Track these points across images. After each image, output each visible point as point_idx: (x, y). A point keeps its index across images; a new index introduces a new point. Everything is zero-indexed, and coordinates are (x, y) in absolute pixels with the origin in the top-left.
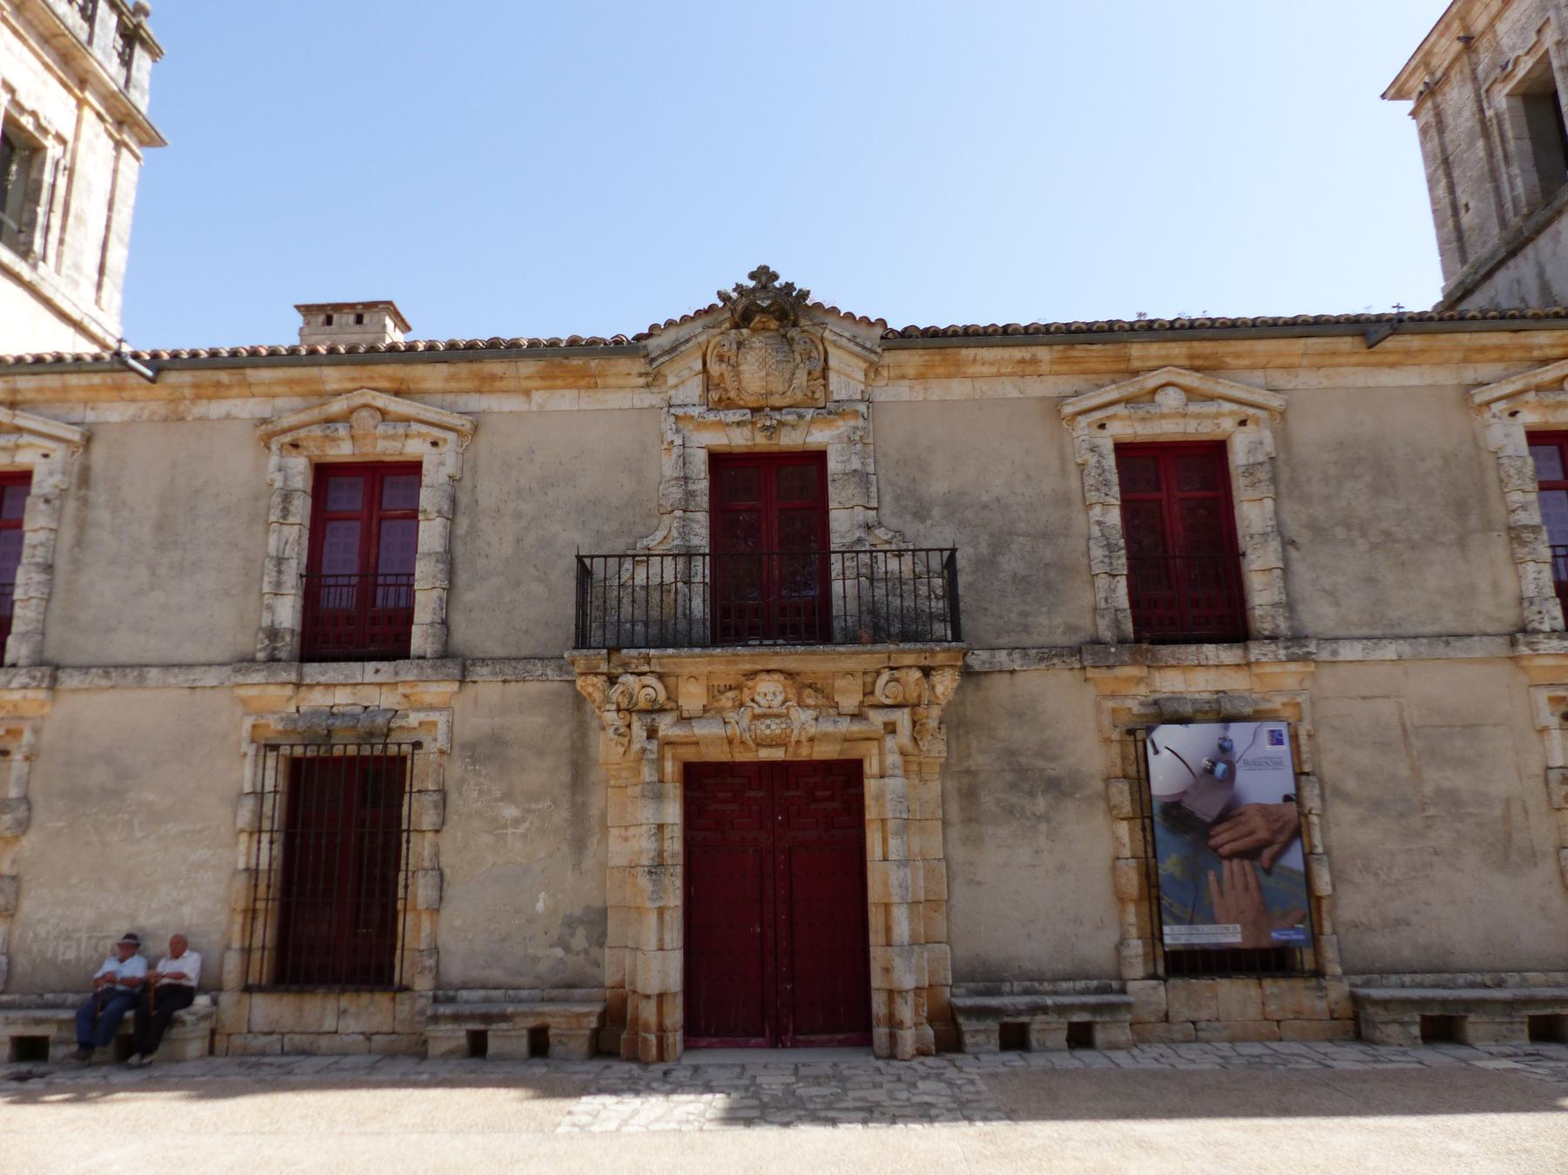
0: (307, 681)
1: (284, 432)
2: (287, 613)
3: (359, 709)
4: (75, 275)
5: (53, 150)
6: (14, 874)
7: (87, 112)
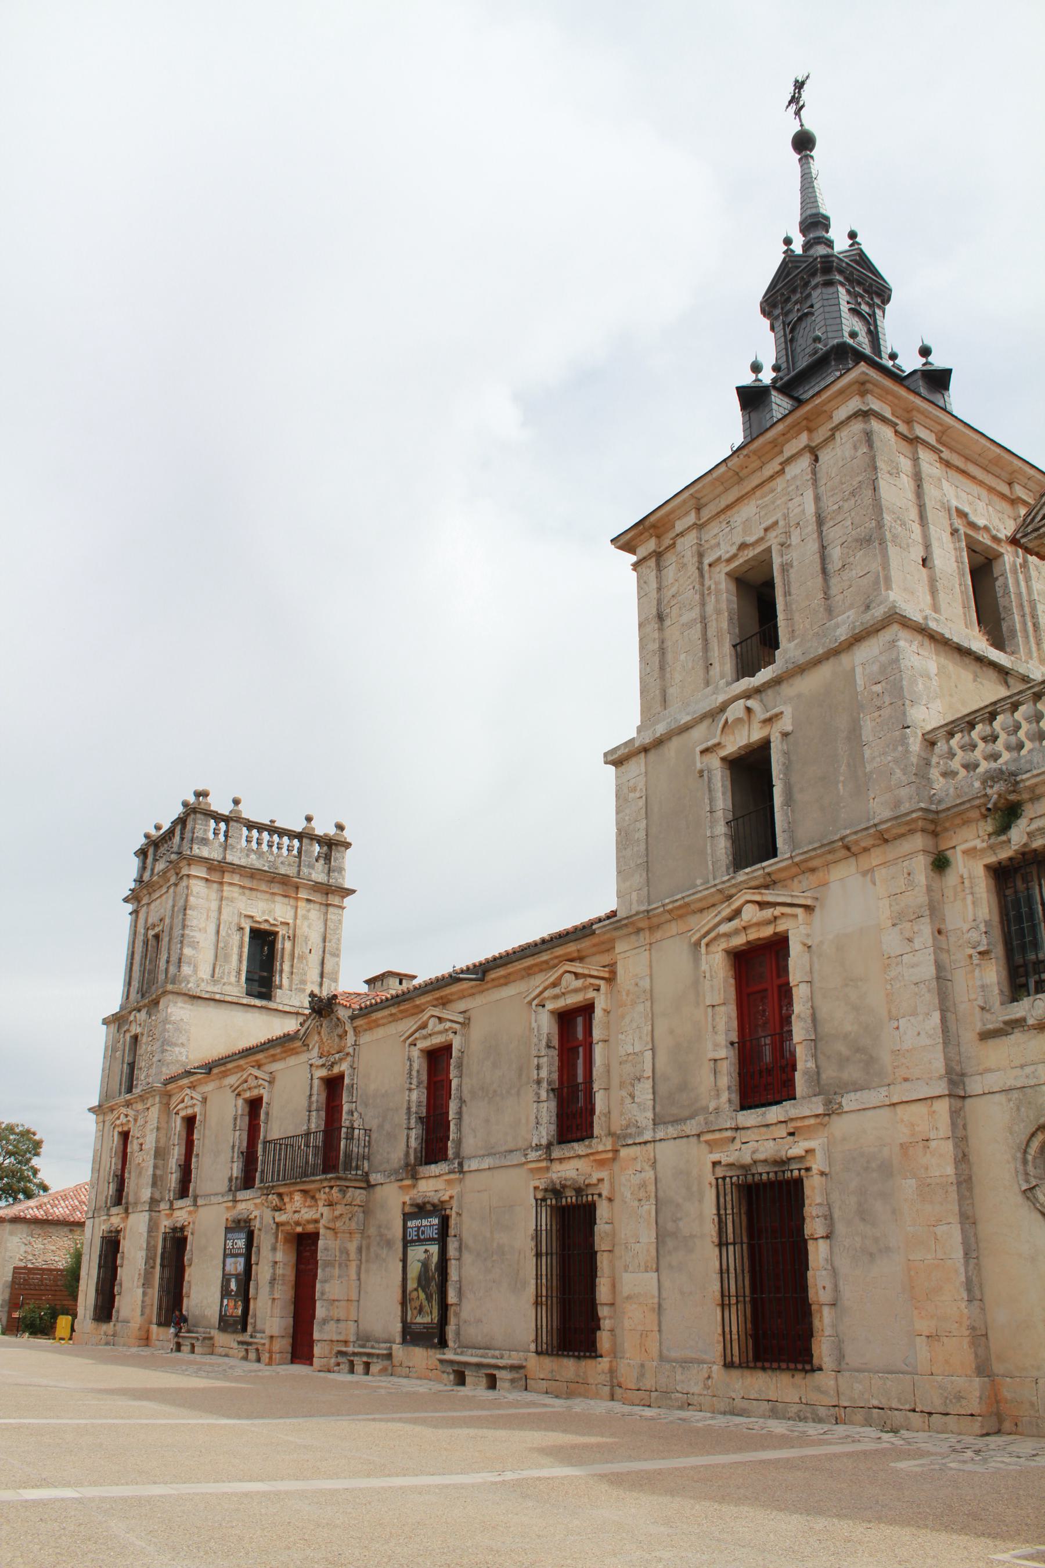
2: (236, 1170)
4: (302, 986)
5: (282, 931)
7: (302, 904)
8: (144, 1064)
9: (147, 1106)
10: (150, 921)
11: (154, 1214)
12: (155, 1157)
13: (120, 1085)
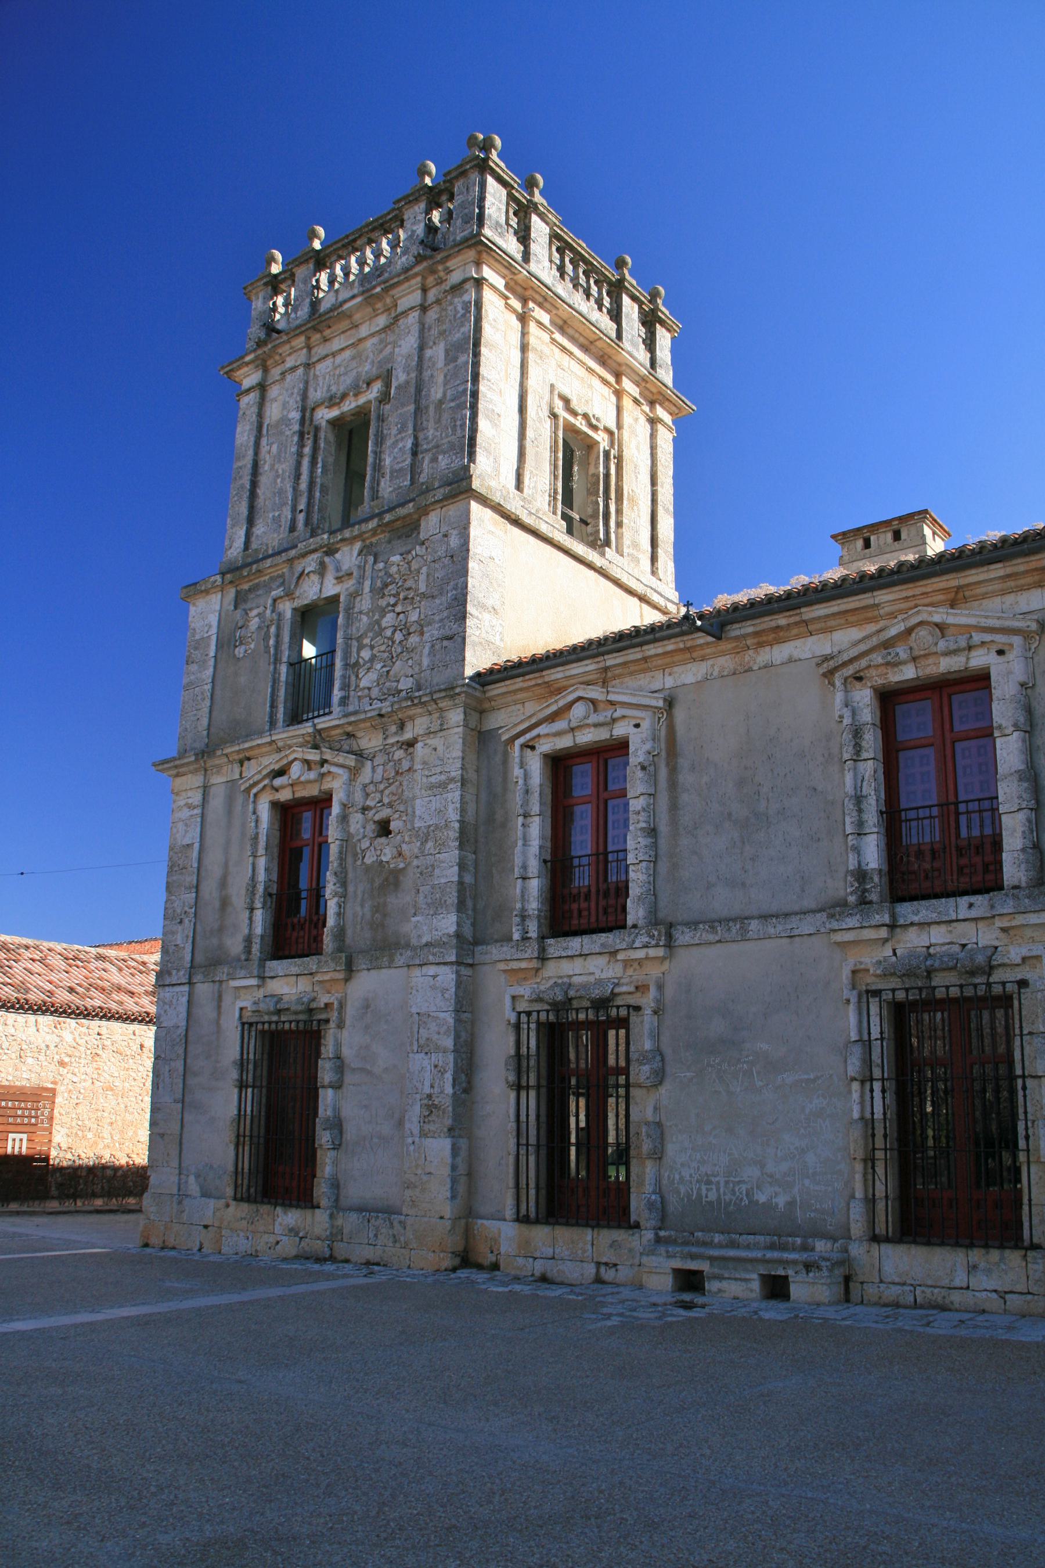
0: (901, 922)
1: (845, 664)
3: (956, 948)
6: (658, 1120)
8: (366, 654)
9: (408, 735)
10: (316, 394)
11: (465, 971)
12: (461, 847)
13: (273, 706)
